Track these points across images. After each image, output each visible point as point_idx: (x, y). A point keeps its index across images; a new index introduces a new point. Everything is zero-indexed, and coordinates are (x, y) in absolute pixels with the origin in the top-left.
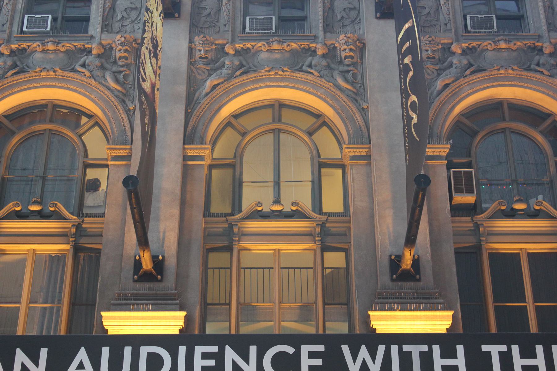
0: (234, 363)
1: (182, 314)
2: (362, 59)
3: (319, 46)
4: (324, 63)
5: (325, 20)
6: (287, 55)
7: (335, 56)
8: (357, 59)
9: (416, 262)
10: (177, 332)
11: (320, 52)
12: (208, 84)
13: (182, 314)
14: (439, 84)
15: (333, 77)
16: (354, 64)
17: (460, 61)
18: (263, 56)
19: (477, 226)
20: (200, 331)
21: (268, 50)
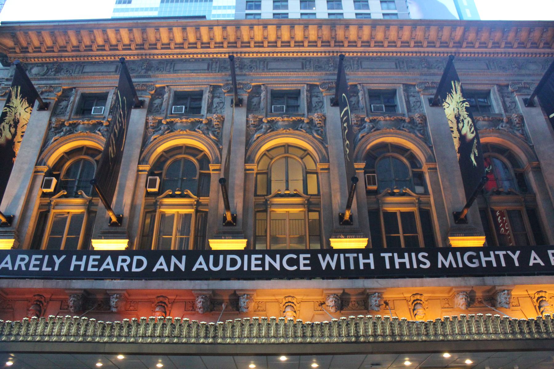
0: (181, 263)
2: (222, 126)
3: (104, 121)
4: (105, 129)
5: (208, 107)
6: (189, 124)
7: (211, 124)
8: (220, 126)
9: (234, 218)
11: (104, 124)
12: (53, 139)
13: (127, 241)
14: (256, 136)
15: (208, 133)
16: (219, 128)
17: (266, 126)
18: (81, 126)
19: (157, 201)
20: (194, 247)
21: (181, 122)
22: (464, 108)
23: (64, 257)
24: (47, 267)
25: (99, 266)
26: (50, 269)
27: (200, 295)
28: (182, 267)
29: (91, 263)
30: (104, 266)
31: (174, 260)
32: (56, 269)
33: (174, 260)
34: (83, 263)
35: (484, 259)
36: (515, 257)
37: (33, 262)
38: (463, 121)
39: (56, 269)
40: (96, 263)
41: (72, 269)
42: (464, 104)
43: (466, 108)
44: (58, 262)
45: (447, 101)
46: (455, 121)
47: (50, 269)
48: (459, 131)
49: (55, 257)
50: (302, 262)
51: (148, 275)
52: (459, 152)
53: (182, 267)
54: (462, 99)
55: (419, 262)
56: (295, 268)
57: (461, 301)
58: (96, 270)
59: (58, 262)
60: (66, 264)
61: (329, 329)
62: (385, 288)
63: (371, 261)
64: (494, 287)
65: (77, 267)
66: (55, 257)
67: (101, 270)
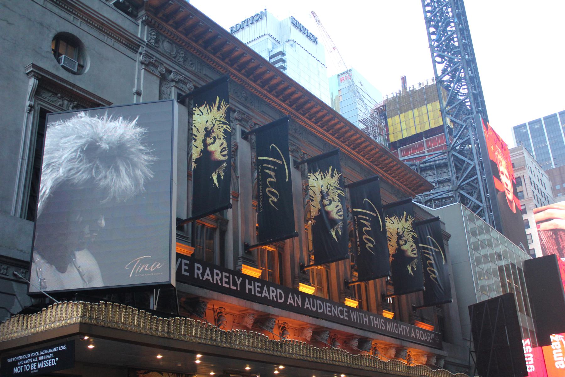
1: (194, 248)
10: (190, 256)
22: (222, 129)
23: (241, 279)
24: (233, 285)
25: (261, 292)
26: (235, 288)
27: (310, 327)
28: (300, 303)
29: (257, 289)
30: (264, 294)
31: (296, 298)
32: (239, 289)
33: (296, 298)
34: (252, 287)
35: (400, 329)
36: (408, 330)
37: (225, 279)
38: (215, 139)
39: (239, 289)
40: (259, 290)
41: (247, 292)
42: (225, 126)
43: (225, 130)
44: (239, 282)
45: (393, 218)
46: (203, 133)
47: (235, 288)
48: (205, 145)
49: (236, 277)
50: (346, 314)
51: (284, 306)
52: (195, 162)
53: (300, 303)
54: (223, 120)
55: (382, 326)
56: (342, 317)
57: (393, 352)
58: (260, 295)
59: (239, 282)
60: (243, 285)
61: (168, 325)
62: (373, 339)
63: (367, 320)
64: (404, 347)
65: (250, 290)
66: (236, 277)
67: (263, 296)
